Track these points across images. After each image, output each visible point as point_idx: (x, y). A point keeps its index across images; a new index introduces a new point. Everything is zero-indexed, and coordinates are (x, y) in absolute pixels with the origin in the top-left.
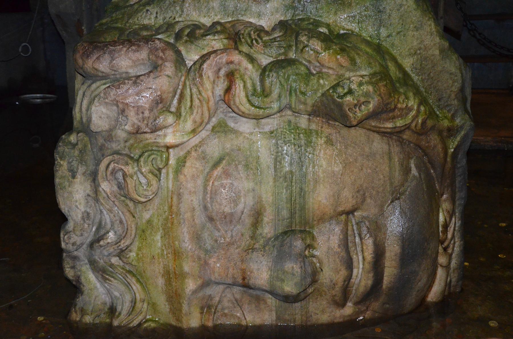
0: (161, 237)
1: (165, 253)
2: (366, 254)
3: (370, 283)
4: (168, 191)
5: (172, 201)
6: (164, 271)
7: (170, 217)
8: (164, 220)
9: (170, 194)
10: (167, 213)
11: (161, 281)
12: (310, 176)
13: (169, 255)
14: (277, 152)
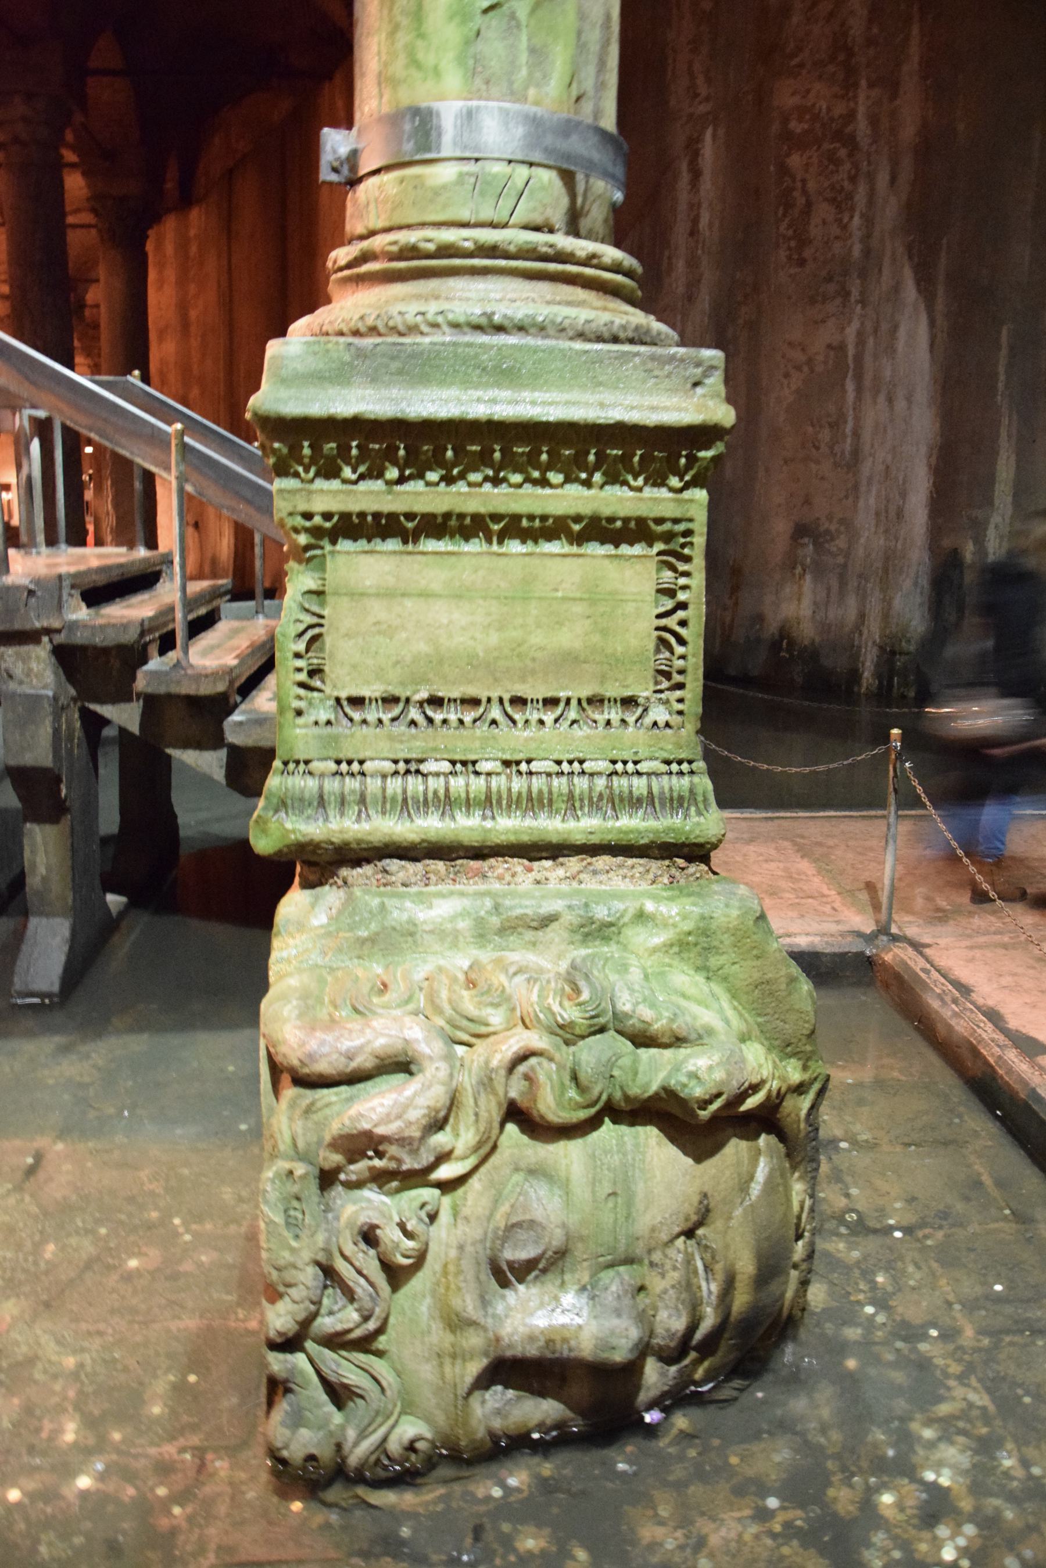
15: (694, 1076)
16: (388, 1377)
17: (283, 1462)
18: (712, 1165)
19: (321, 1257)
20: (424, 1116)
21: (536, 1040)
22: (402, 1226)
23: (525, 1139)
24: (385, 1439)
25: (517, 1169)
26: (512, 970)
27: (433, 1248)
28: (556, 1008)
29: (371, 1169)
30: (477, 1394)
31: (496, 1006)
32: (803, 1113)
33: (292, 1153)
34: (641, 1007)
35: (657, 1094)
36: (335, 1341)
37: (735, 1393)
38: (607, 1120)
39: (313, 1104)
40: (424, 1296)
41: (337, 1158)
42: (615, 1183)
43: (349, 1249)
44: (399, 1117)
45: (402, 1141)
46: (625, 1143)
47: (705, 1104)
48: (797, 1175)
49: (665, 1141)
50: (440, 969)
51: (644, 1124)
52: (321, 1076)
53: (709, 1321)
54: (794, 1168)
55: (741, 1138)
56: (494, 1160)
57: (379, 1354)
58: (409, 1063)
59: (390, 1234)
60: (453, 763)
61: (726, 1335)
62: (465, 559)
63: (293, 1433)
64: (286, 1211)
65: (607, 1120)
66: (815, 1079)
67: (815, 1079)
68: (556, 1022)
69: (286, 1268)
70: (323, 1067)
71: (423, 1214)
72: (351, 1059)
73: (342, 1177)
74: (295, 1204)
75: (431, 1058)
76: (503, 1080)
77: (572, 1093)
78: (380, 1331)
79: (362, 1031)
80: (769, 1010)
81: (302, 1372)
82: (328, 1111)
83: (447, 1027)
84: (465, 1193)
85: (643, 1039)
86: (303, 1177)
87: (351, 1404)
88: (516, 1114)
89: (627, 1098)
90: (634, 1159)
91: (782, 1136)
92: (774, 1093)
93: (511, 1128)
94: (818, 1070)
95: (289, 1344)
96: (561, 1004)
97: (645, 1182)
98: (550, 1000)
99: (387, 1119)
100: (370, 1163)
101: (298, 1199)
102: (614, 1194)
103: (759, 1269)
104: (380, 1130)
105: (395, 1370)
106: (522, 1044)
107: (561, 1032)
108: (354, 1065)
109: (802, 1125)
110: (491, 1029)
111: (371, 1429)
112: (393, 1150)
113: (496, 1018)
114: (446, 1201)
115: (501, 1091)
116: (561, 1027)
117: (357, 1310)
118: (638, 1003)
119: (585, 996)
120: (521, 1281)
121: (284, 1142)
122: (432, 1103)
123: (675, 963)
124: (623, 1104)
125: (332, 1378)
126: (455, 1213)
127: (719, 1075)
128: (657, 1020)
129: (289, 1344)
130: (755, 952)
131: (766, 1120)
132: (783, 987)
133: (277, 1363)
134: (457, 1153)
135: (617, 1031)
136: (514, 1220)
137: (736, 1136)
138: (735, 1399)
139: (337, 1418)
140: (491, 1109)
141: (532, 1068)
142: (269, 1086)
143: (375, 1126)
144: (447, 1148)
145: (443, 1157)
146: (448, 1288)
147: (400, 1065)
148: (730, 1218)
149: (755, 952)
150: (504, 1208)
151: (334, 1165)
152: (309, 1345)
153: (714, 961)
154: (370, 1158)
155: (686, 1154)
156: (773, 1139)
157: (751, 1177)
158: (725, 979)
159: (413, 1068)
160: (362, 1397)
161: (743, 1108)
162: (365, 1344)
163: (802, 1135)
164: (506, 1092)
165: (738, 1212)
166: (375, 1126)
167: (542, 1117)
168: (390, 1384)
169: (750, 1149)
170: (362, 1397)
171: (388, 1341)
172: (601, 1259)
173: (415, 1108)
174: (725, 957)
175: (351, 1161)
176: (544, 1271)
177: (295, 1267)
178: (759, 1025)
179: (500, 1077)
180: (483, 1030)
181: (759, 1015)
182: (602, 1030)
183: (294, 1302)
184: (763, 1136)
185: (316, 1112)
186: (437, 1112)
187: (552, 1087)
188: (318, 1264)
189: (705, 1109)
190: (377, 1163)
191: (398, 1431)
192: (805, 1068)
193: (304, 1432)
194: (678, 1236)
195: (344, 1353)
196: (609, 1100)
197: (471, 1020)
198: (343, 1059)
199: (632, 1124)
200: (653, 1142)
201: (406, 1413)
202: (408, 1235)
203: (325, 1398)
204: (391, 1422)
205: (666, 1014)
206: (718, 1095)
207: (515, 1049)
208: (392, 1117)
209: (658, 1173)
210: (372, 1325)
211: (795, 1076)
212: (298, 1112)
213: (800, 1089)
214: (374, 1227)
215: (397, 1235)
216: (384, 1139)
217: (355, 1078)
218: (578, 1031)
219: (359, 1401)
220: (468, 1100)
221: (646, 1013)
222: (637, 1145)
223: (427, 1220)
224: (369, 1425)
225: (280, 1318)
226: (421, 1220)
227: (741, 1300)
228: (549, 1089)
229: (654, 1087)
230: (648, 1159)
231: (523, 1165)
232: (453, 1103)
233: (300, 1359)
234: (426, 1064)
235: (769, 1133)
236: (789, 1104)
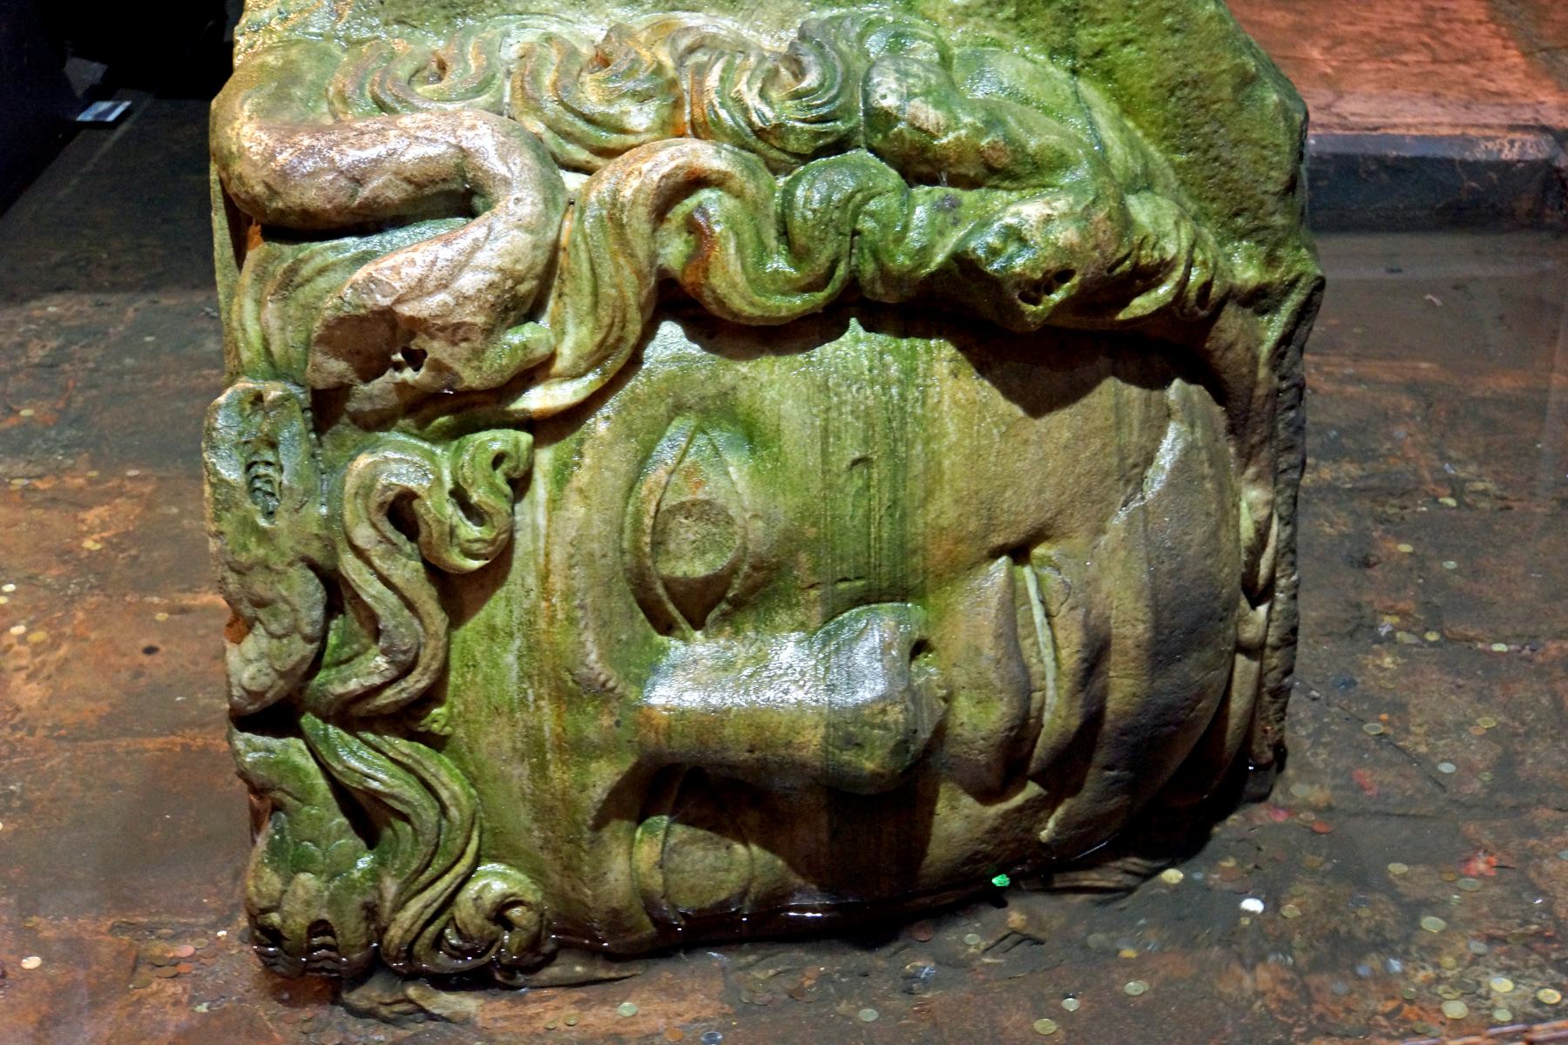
0: (519, 658)
1: (531, 698)
2: (1064, 653)
3: (1075, 722)
4: (535, 538)
5: (548, 561)
6: (527, 744)
7: (544, 604)
8: (528, 612)
9: (541, 544)
10: (533, 595)
11: (519, 773)
12: (918, 467)
13: (542, 703)
14: (828, 410)
15: (1014, 235)
16: (450, 782)
17: (273, 935)
18: (1061, 424)
19: (315, 551)
20: (491, 285)
21: (709, 157)
22: (459, 496)
23: (695, 349)
24: (450, 900)
25: (678, 409)
26: (685, 42)
27: (523, 542)
28: (752, 99)
29: (402, 386)
30: (619, 827)
31: (641, 97)
32: (1265, 350)
33: (263, 365)
34: (916, 102)
35: (943, 270)
36: (354, 715)
37: (1129, 880)
38: (853, 321)
39: (293, 271)
40: (511, 635)
41: (337, 367)
42: (866, 441)
43: (363, 535)
44: (443, 286)
45: (455, 332)
46: (885, 367)
47: (1036, 289)
48: (1251, 471)
49: (968, 370)
50: (549, 38)
51: (927, 335)
52: (305, 213)
53: (1057, 712)
54: (1247, 457)
55: (1129, 379)
56: (636, 384)
57: (437, 742)
58: (470, 193)
59: (438, 509)
61: (1100, 757)
63: (288, 881)
64: (249, 467)
65: (853, 321)
66: (1293, 284)
67: (1293, 284)
68: (750, 124)
69: (250, 568)
70: (312, 195)
71: (499, 477)
72: (358, 182)
73: (352, 406)
74: (269, 456)
75: (506, 182)
76: (646, 228)
77: (779, 263)
78: (432, 695)
79: (380, 132)
80: (1197, 140)
81: (296, 769)
82: (322, 283)
83: (548, 136)
84: (581, 442)
85: (919, 164)
86: (280, 403)
87: (388, 832)
88: (674, 298)
89: (884, 273)
90: (902, 397)
91: (1220, 393)
92: (1193, 295)
93: (671, 334)
94: (1299, 267)
95: (274, 715)
96: (762, 94)
97: (926, 443)
98: (742, 86)
99: (420, 289)
100: (399, 376)
101: (273, 446)
102: (864, 461)
103: (1157, 627)
104: (406, 310)
105: (465, 771)
106: (680, 161)
107: (761, 145)
108: (365, 193)
109: (1263, 372)
110: (631, 140)
111: (424, 878)
112: (437, 349)
113: (640, 117)
114: (545, 458)
115: (641, 253)
116: (760, 133)
117: (384, 652)
118: (911, 96)
119: (811, 80)
120: (698, 624)
121: (248, 343)
122: (506, 262)
123: (1008, 38)
124: (879, 289)
125: (351, 782)
126: (562, 476)
127: (1066, 235)
128: (948, 129)
129: (274, 715)
130: (1168, 20)
131: (1176, 347)
132: (1227, 92)
133: (253, 748)
134: (559, 365)
135: (872, 150)
136: (671, 500)
137: (1115, 373)
138: (1129, 890)
139: (365, 862)
140: (627, 287)
141: (700, 207)
142: (230, 252)
143: (399, 301)
144: (541, 351)
145: (535, 371)
146: (552, 620)
147: (454, 196)
148: (1100, 531)
149: (1168, 20)
150: (657, 475)
151: (332, 380)
152: (308, 721)
153: (1087, 38)
154: (398, 367)
155: (1009, 394)
156: (1197, 392)
157: (1149, 460)
158: (1108, 75)
159: (477, 202)
160: (405, 818)
161: (1121, 316)
162: (406, 719)
163: (1260, 391)
164: (653, 256)
165: (1119, 519)
166: (399, 301)
167: (720, 302)
168: (454, 796)
169: (1147, 403)
170: (405, 818)
171: (450, 719)
172: (842, 586)
173: (476, 269)
174: (1106, 29)
175: (368, 376)
176: (738, 604)
177: (267, 567)
178: (1177, 168)
179: (639, 222)
180: (614, 140)
181: (1177, 149)
182: (840, 145)
183: (272, 635)
184: (1177, 382)
185: (301, 285)
186: (519, 280)
187: (740, 248)
188: (312, 566)
189: (1036, 302)
190: (408, 375)
191: (472, 889)
192: (1271, 261)
193: (305, 878)
194: (995, 554)
195: (370, 737)
196: (853, 283)
197: (590, 120)
198: (343, 182)
199: (904, 334)
200: (942, 368)
201: (494, 859)
202: (473, 513)
203: (342, 819)
204: (461, 868)
205: (967, 120)
206: (1064, 275)
207: (665, 170)
208: (430, 284)
209: (951, 428)
210: (416, 682)
211: (1246, 272)
212: (270, 287)
213: (1259, 300)
214: (407, 497)
215: (452, 512)
216: (416, 325)
217: (370, 220)
218: (793, 145)
219: (399, 824)
220: (577, 264)
221: (929, 115)
222: (910, 372)
223: (507, 489)
224: (421, 871)
225: (250, 665)
226: (494, 488)
227: (1123, 688)
228: (732, 250)
229: (939, 258)
230: (931, 401)
231: (690, 397)
232: (549, 273)
233: (294, 750)
234: (500, 191)
235: (1190, 379)
236: (1232, 322)
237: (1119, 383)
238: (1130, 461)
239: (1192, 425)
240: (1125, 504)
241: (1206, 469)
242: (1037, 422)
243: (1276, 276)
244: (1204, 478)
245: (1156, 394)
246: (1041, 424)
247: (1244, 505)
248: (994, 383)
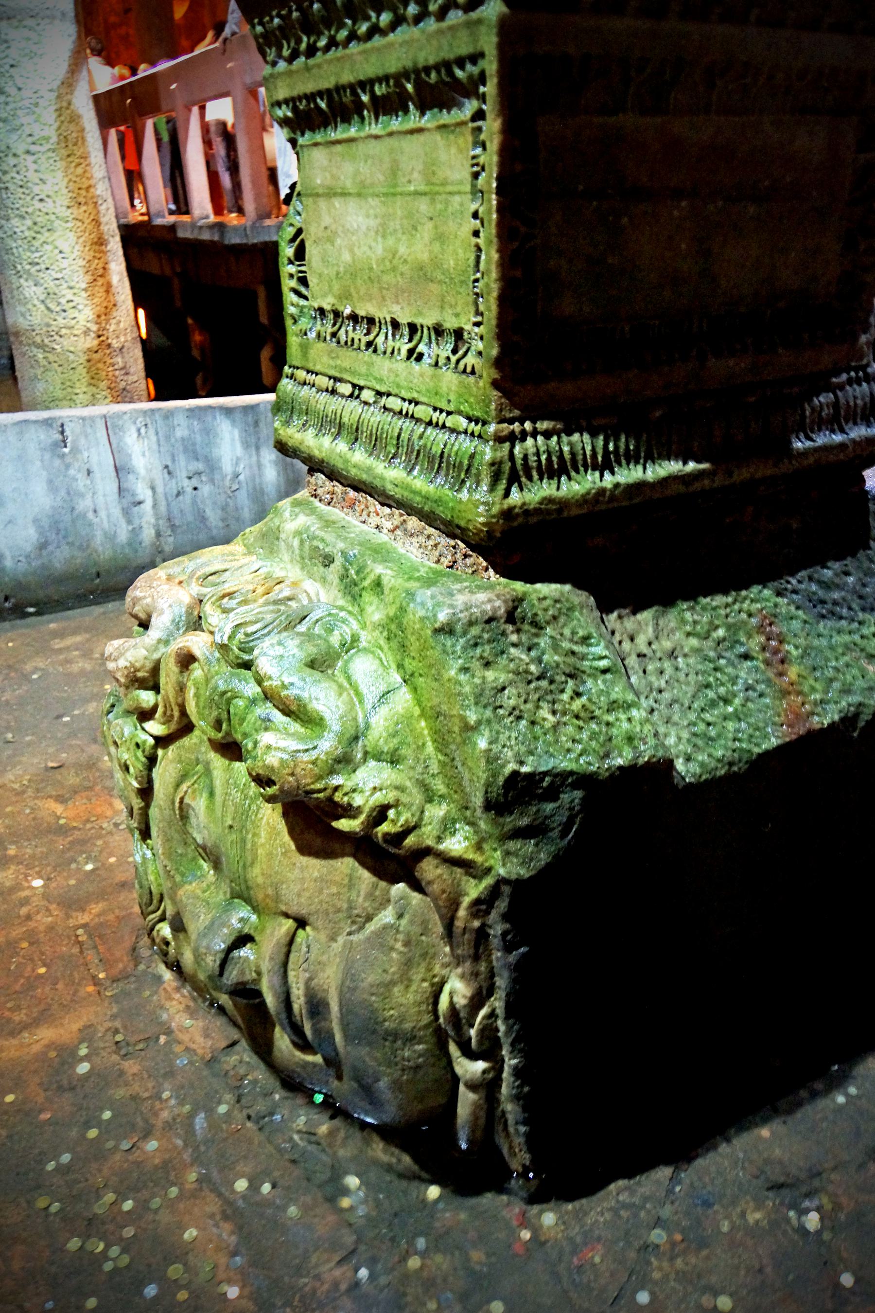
32: (466, 901)
48: (459, 970)
60: (354, 386)
62: (361, 148)
66: (489, 870)
109: (462, 913)
155: (291, 832)
157: (369, 918)
161: (335, 824)
165: (341, 940)
169: (375, 886)
181: (440, 751)
184: (401, 885)
211: (457, 844)
230: (260, 816)
237: (357, 864)
238: (356, 912)
239: (400, 916)
240: (349, 934)
241: (399, 946)
242: (301, 857)
243: (478, 858)
244: (392, 949)
245: (383, 884)
246: (305, 860)
247: (447, 989)
248: (287, 823)
